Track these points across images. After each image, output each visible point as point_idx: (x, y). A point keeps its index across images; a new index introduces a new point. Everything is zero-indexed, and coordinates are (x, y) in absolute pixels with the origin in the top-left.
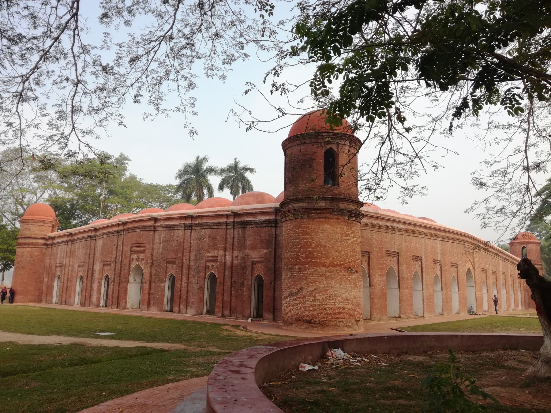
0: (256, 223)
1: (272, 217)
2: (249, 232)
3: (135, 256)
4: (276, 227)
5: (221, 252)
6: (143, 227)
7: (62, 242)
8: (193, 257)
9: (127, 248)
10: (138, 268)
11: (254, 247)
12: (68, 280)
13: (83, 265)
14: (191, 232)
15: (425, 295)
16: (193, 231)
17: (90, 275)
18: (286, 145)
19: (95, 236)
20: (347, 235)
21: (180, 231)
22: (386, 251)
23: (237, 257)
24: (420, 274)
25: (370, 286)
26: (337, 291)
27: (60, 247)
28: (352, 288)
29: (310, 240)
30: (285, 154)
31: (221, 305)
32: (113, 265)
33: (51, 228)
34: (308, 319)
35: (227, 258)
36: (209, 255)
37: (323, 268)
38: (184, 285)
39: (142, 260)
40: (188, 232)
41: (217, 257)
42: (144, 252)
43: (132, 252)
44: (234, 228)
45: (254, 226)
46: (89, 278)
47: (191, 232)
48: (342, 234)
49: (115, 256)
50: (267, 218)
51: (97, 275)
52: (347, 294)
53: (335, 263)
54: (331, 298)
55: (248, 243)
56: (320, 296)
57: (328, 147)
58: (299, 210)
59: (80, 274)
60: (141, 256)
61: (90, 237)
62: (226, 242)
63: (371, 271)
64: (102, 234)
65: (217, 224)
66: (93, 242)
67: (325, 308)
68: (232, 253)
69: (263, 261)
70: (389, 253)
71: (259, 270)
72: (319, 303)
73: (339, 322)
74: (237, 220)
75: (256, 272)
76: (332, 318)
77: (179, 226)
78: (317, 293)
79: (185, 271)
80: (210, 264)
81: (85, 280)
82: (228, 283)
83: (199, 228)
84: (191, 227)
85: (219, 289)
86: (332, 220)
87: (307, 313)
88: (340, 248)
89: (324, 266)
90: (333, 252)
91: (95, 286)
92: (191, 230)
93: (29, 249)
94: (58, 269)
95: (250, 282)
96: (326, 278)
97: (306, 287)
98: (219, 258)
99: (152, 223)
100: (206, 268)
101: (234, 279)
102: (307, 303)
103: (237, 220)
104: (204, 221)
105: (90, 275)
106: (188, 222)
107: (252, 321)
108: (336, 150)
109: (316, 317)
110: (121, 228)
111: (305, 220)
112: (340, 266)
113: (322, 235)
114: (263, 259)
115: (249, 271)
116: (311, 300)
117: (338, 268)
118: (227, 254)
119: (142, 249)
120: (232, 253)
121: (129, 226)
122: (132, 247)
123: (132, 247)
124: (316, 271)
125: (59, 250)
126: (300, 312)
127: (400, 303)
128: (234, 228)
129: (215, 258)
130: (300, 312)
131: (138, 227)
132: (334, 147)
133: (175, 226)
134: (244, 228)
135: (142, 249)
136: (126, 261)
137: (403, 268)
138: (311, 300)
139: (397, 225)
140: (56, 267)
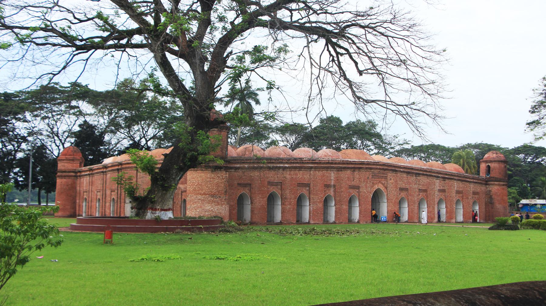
7: (86, 175)
19: (106, 172)
27: (85, 178)
32: (116, 191)
46: (104, 200)
48: (210, 178)
51: (108, 199)
59: (98, 197)
61: (103, 172)
64: (110, 171)
66: (105, 176)
81: (101, 201)
91: (108, 204)
93: (65, 180)
94: (85, 194)
115: (180, 196)
131: (128, 168)
140: (84, 192)
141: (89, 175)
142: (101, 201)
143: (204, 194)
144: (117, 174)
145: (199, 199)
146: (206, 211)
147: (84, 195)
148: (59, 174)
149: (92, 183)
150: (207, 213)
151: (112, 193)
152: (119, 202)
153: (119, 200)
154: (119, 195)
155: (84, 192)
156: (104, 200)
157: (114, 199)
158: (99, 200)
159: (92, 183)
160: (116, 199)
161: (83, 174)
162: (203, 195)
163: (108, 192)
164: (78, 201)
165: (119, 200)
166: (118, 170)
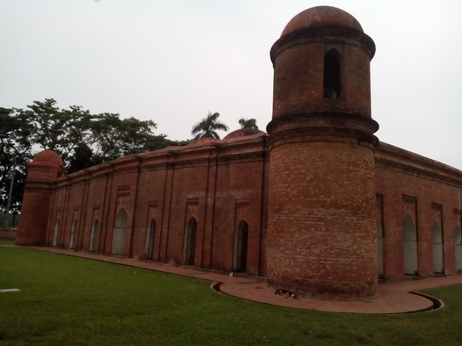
0: (240, 157)
1: (260, 149)
2: (233, 167)
3: (121, 199)
4: (264, 161)
5: (203, 194)
6: (129, 169)
7: (62, 187)
8: (174, 200)
9: (114, 192)
10: (123, 210)
11: (238, 187)
12: (65, 224)
13: (77, 210)
14: (173, 172)
15: (445, 249)
16: (175, 171)
17: (83, 218)
18: (276, 53)
19: (89, 180)
20: (356, 165)
21: (162, 171)
22: (403, 195)
23: (219, 198)
24: (440, 224)
25: (383, 236)
26: (341, 241)
27: (61, 192)
28: (363, 237)
29: (303, 171)
30: (274, 67)
31: (201, 255)
32: (101, 209)
33: (56, 174)
34: (299, 278)
35: (209, 200)
36: (190, 196)
37: (322, 209)
38: (165, 230)
39: (127, 203)
40: (170, 172)
41: (198, 199)
42: (128, 195)
43: (119, 195)
44: (217, 165)
45: (239, 161)
46: (82, 222)
47: (173, 172)
48: (349, 164)
49: (103, 199)
50: (254, 150)
51: (89, 220)
52: (355, 247)
53: (339, 202)
54: (332, 252)
55: (232, 182)
56: (317, 247)
57: (330, 47)
58: (289, 131)
59: (75, 218)
60: (127, 199)
61: (84, 180)
62: (208, 183)
63: (385, 219)
65: (198, 161)
67: (324, 265)
68: (215, 194)
69: (248, 204)
70: (406, 198)
71: (243, 215)
72: (315, 258)
73: (344, 284)
74: (220, 155)
75: (241, 217)
76: (334, 279)
77: (161, 165)
78: (312, 243)
79: (166, 216)
80: (190, 208)
81: (78, 224)
82: (209, 229)
83: (181, 167)
84: (172, 166)
85: (199, 235)
86: (334, 144)
87: (298, 270)
88: (346, 183)
89: (323, 206)
90: (336, 188)
91: (87, 229)
92: (174, 169)
94: (59, 213)
95: (232, 228)
96: (325, 222)
97: (297, 235)
98: (200, 201)
99: (137, 164)
100: (187, 211)
101: (215, 225)
102: (298, 257)
103: (220, 155)
104: (187, 158)
105: (83, 218)
106: (171, 160)
107: (234, 276)
108: (341, 51)
109: (311, 278)
110: (110, 170)
111: (297, 145)
112: (346, 207)
113: (320, 164)
114: (247, 201)
115: (231, 216)
116: (304, 253)
117: (343, 210)
118: (209, 195)
119: (127, 191)
120: (215, 194)
121: (117, 168)
122: (118, 190)
123: (118, 190)
124: (312, 212)
125: (60, 194)
126: (288, 270)
127: (418, 258)
128: (217, 165)
129: (196, 201)
130: (288, 270)
131: (124, 169)
132: (338, 48)
133: (157, 166)
134: (228, 164)
135: (127, 191)
136: (113, 205)
137: (422, 217)
138: (304, 253)
139: (415, 166)
140: (57, 211)
141: (66, 186)
142: (78, 224)
143: (334, 205)
144: (105, 181)
145: (320, 220)
146: (338, 255)
147: (57, 215)
148: (27, 185)
149: (68, 198)
150: (342, 260)
151: (96, 212)
152: (104, 226)
153: (105, 223)
154: (105, 216)
155: (57, 211)
156: (82, 222)
157: (97, 221)
158: (76, 222)
159: (68, 198)
160: (100, 220)
161: (59, 185)
162: (330, 206)
163: (90, 210)
164: (49, 223)
165: (105, 223)
166: (107, 174)
